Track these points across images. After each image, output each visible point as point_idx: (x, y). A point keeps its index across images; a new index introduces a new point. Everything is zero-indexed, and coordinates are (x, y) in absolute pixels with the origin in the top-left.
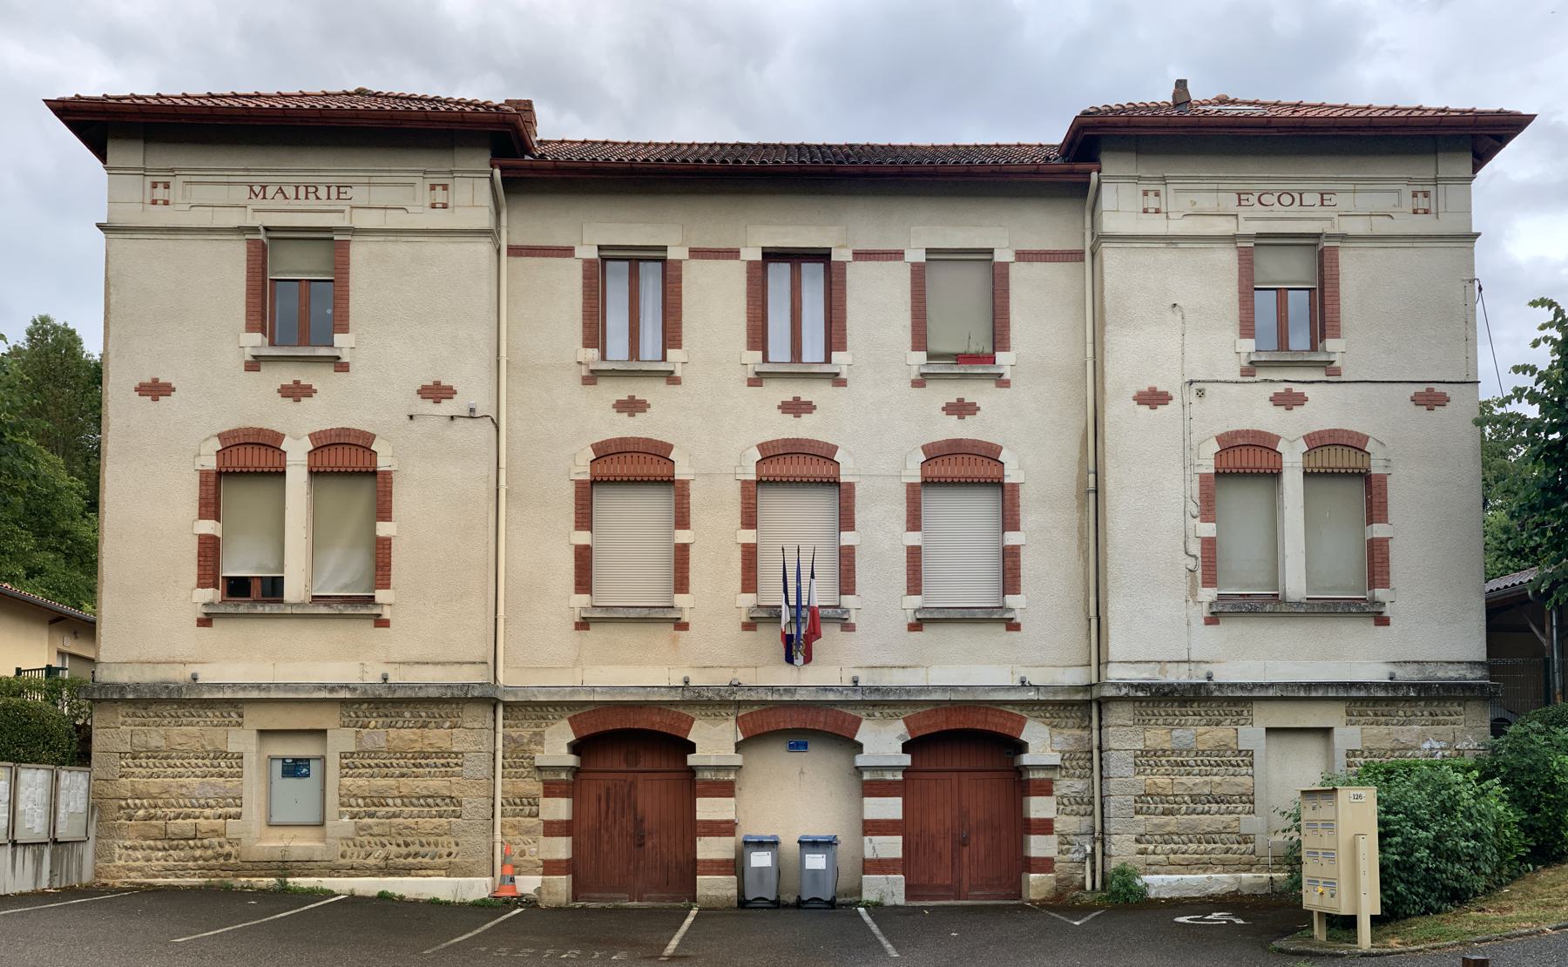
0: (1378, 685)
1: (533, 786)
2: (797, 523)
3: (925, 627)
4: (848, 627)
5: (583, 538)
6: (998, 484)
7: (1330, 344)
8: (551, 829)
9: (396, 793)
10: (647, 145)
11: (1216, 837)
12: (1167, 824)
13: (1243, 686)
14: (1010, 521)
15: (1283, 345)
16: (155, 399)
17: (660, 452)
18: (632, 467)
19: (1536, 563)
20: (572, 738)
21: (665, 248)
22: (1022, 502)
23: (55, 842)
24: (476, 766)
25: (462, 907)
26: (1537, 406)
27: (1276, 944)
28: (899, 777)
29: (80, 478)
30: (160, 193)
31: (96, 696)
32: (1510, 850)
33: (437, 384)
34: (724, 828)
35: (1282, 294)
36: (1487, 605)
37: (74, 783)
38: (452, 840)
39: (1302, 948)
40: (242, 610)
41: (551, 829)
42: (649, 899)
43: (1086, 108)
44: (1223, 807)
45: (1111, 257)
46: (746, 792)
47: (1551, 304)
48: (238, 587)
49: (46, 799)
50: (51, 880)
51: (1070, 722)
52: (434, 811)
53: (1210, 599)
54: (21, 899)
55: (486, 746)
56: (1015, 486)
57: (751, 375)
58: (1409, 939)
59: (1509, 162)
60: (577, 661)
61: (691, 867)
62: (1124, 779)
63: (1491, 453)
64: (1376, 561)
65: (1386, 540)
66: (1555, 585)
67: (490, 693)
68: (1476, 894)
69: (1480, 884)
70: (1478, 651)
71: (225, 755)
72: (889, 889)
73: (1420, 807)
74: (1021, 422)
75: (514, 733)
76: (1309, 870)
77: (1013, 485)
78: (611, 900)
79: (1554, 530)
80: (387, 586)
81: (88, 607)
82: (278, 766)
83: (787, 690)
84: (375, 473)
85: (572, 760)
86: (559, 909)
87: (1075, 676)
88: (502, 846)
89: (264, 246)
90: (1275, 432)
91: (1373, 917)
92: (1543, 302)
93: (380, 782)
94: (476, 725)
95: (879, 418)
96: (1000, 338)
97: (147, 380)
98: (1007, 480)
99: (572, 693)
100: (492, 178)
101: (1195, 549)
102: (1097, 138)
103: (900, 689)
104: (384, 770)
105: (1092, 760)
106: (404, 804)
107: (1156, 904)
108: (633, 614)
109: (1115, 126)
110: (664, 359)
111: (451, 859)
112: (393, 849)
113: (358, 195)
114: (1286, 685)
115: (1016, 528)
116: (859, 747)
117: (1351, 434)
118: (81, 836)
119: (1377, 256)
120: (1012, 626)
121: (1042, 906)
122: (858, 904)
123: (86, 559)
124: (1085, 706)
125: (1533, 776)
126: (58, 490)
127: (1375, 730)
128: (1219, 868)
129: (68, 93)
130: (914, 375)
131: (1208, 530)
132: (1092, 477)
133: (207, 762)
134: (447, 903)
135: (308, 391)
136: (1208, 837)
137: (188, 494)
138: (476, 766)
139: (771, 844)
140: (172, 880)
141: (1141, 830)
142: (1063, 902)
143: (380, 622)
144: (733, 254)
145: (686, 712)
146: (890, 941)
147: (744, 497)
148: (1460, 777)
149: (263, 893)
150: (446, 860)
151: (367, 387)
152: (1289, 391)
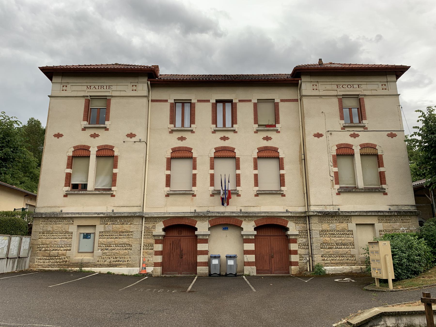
0: (386, 212)
1: (152, 241)
2: (225, 168)
4: (239, 195)
5: (168, 172)
6: (278, 158)
7: (364, 121)
8: (157, 253)
9: (114, 243)
10: (187, 75)
13: (348, 212)
14: (281, 167)
15: (352, 122)
18: (182, 154)
19: (424, 178)
20: (163, 227)
21: (191, 100)
23: (19, 257)
24: (136, 235)
25: (131, 276)
26: (421, 137)
27: (365, 288)
28: (254, 238)
29: (37, 158)
31: (35, 216)
33: (131, 133)
34: (205, 253)
35: (350, 109)
36: (414, 189)
37: (26, 240)
38: (129, 257)
39: (373, 289)
40: (76, 192)
41: (157, 253)
42: (183, 274)
44: (346, 246)
45: (305, 100)
46: (211, 242)
47: (421, 111)
48: (75, 187)
49: (18, 245)
50: (17, 269)
52: (124, 248)
53: (338, 188)
54: (8, 274)
55: (140, 230)
56: (282, 158)
57: (213, 131)
58: (404, 286)
59: (404, 78)
60: (166, 205)
61: (196, 264)
62: (317, 238)
63: (409, 148)
64: (382, 177)
65: (384, 172)
66: (431, 184)
67: (141, 215)
68: (421, 272)
69: (422, 269)
70: (414, 203)
71: (67, 232)
72: (251, 270)
73: (402, 247)
74: (283, 141)
75: (147, 226)
76: (373, 265)
79: (429, 169)
80: (115, 186)
81: (35, 192)
82: (82, 235)
83: (222, 213)
84: (114, 156)
85: (163, 233)
87: (301, 209)
88: (142, 258)
89: (89, 100)
90: (352, 144)
91: (393, 280)
92: (418, 111)
93: (109, 240)
94: (137, 223)
96: (277, 121)
97: (57, 133)
100: (148, 84)
101: (333, 174)
102: (300, 72)
103: (253, 212)
104: (111, 236)
105: (307, 233)
106: (116, 246)
107: (328, 275)
109: (304, 69)
110: (190, 127)
111: (128, 262)
112: (112, 259)
113: (114, 88)
114: (360, 211)
115: (283, 169)
116: (242, 229)
117: (372, 144)
118: (26, 255)
120: (283, 195)
121: (295, 276)
122: (243, 275)
123: (36, 179)
124: (305, 217)
125: (433, 238)
126: (31, 161)
127: (386, 224)
128: (346, 265)
129: (45, 65)
130: (255, 130)
131: (336, 169)
132: (303, 156)
133: (63, 234)
134: (127, 275)
135: (97, 136)
136: (342, 255)
137: (65, 161)
139: (218, 257)
140: (50, 269)
141: (323, 253)
142: (301, 275)
143: (113, 196)
144: (208, 101)
146: (253, 286)
147: (211, 161)
149: (75, 272)
150: (127, 262)
151: (112, 135)
152: (354, 133)
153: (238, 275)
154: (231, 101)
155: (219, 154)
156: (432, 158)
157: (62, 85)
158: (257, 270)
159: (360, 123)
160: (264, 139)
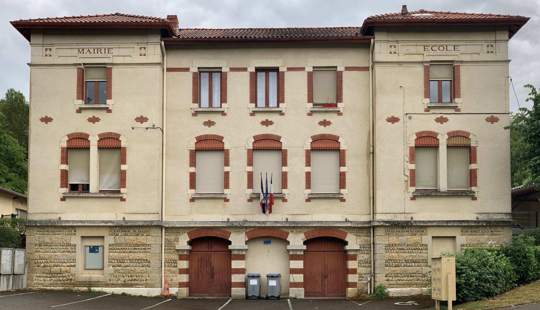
0: (472, 221)
1: (175, 257)
2: (267, 163)
3: (311, 200)
4: (285, 200)
5: (193, 170)
6: (338, 150)
7: (457, 100)
8: (182, 271)
11: (414, 275)
12: (396, 270)
13: (424, 222)
14: (342, 163)
15: (440, 100)
16: (46, 123)
17: (219, 139)
18: (210, 145)
20: (189, 239)
21: (221, 68)
22: (346, 156)
23: (14, 274)
24: (155, 249)
25: (151, 298)
28: (302, 253)
30: (48, 52)
31: (27, 225)
32: (510, 279)
33: (142, 117)
34: (241, 271)
35: (440, 82)
37: (20, 254)
40: (75, 195)
41: (182, 271)
42: (215, 296)
43: (369, 16)
44: (417, 264)
45: (378, 69)
48: (74, 187)
49: (11, 260)
50: (12, 287)
51: (363, 235)
53: (413, 191)
55: (159, 242)
56: (344, 151)
57: (251, 112)
60: (190, 213)
61: (230, 285)
64: (472, 177)
67: (160, 224)
70: (508, 209)
71: (70, 245)
72: (299, 293)
74: (346, 128)
75: (168, 238)
77: (343, 150)
78: (202, 296)
80: (125, 187)
82: (88, 249)
83: (263, 222)
84: (120, 148)
85: (188, 247)
86: (184, 299)
87: (365, 218)
89: (83, 70)
90: (436, 131)
93: (122, 255)
94: (155, 235)
95: (296, 127)
96: (339, 98)
97: (44, 117)
98: (341, 149)
99: (188, 224)
101: (408, 173)
103: (302, 222)
104: (124, 250)
105: (371, 247)
106: (130, 262)
108: (210, 196)
109: (379, 23)
110: (221, 107)
111: (147, 281)
112: (127, 278)
113: (115, 52)
114: (439, 221)
115: (344, 165)
116: (288, 243)
117: (464, 132)
118: (21, 272)
119: (474, 68)
120: (343, 200)
122: (288, 298)
124: (368, 229)
127: (471, 237)
128: (415, 286)
130: (308, 111)
131: (413, 167)
132: (371, 148)
133: (64, 247)
134: (145, 297)
135: (98, 120)
136: (411, 275)
138: (155, 249)
139: (257, 277)
140: (52, 288)
141: (387, 272)
142: (359, 298)
143: (123, 200)
144: (245, 69)
147: (248, 155)
148: (490, 253)
150: (145, 282)
151: (118, 118)
152: (442, 117)
153: (282, 298)
154: (276, 69)
155: (260, 145)
156: (536, 151)
157: (44, 48)
159: (451, 102)
160: (321, 123)
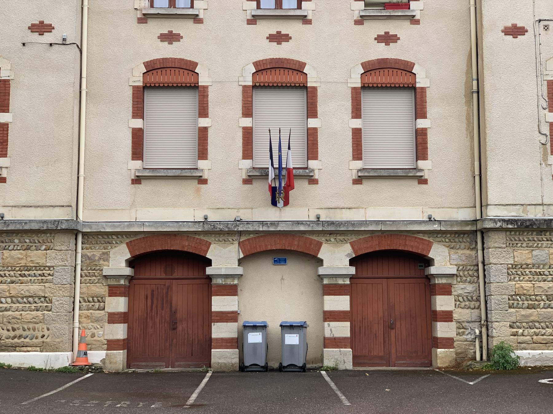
1: (102, 289)
2: (279, 113)
3: (364, 181)
4: (313, 181)
5: (138, 123)
6: (412, 88)
8: (113, 318)
9: (7, 294)
12: (531, 315)
14: (420, 112)
18: (170, 78)
20: (129, 256)
24: (62, 276)
28: (348, 282)
33: (42, 22)
34: (230, 317)
38: (45, 327)
41: (113, 318)
42: (179, 366)
46: (246, 292)
51: (463, 245)
52: (33, 306)
55: (70, 262)
56: (423, 89)
57: (249, 17)
60: (133, 205)
61: (208, 343)
62: (500, 283)
67: (73, 226)
72: (341, 358)
75: (89, 253)
78: (154, 367)
83: (273, 223)
85: (128, 271)
86: (117, 373)
87: (465, 215)
88: (78, 329)
98: (418, 85)
99: (128, 226)
101: (546, 130)
105: (479, 270)
106: (12, 302)
110: (192, 7)
111: (44, 339)
115: (424, 116)
120: (422, 181)
121: (445, 371)
122: (321, 368)
124: (472, 234)
130: (356, 16)
132: (475, 83)
134: (41, 370)
139: (262, 327)
141: (513, 319)
142: (461, 369)
145: (206, 238)
146: (344, 394)
147: (244, 97)
153: (310, 369)
155: (265, 78)
158: (354, 357)
